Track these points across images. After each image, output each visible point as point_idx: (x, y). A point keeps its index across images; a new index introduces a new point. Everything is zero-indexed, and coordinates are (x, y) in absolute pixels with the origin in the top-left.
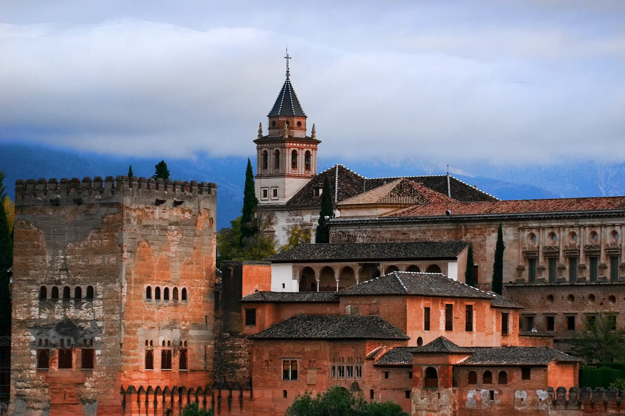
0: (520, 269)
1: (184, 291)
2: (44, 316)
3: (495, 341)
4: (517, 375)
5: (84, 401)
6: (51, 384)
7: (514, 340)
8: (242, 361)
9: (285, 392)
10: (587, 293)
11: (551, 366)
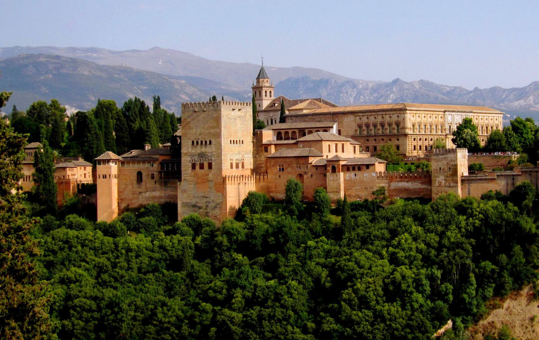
0: (356, 131)
1: (242, 141)
2: (193, 151)
3: (352, 156)
4: (365, 168)
5: (209, 181)
6: (196, 175)
7: (358, 155)
8: (263, 165)
9: (280, 176)
10: (381, 138)
11: (377, 164)
